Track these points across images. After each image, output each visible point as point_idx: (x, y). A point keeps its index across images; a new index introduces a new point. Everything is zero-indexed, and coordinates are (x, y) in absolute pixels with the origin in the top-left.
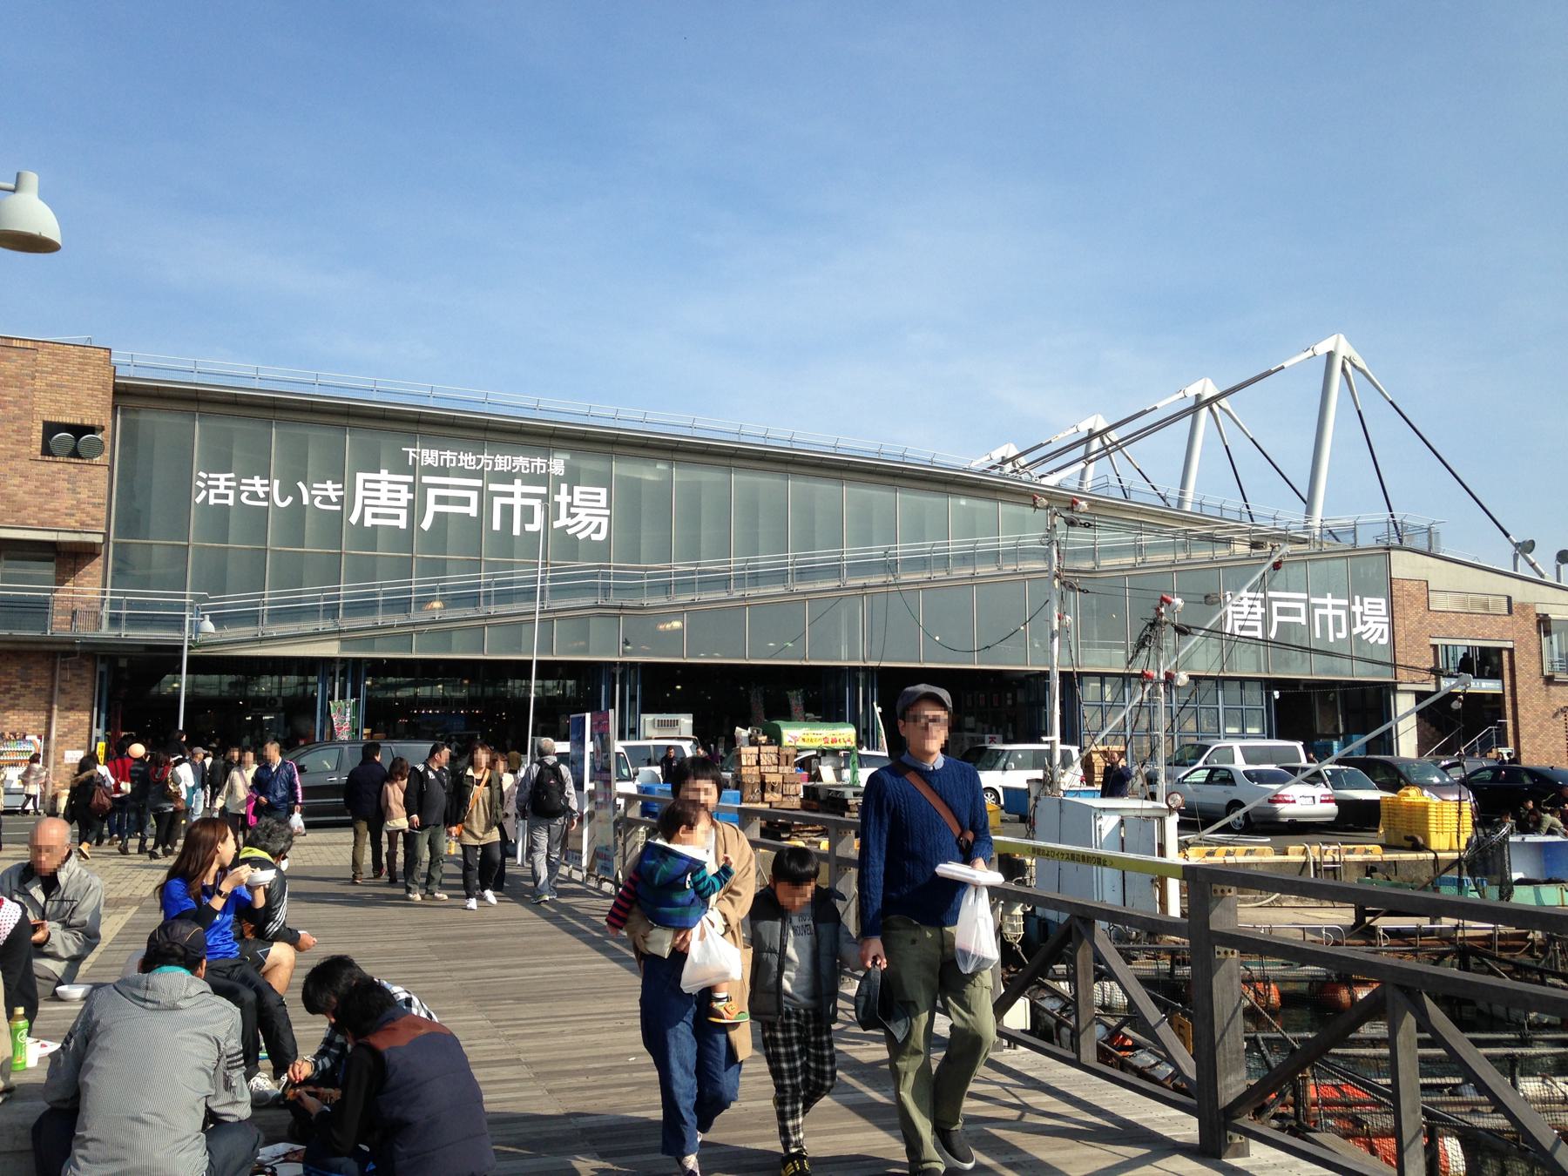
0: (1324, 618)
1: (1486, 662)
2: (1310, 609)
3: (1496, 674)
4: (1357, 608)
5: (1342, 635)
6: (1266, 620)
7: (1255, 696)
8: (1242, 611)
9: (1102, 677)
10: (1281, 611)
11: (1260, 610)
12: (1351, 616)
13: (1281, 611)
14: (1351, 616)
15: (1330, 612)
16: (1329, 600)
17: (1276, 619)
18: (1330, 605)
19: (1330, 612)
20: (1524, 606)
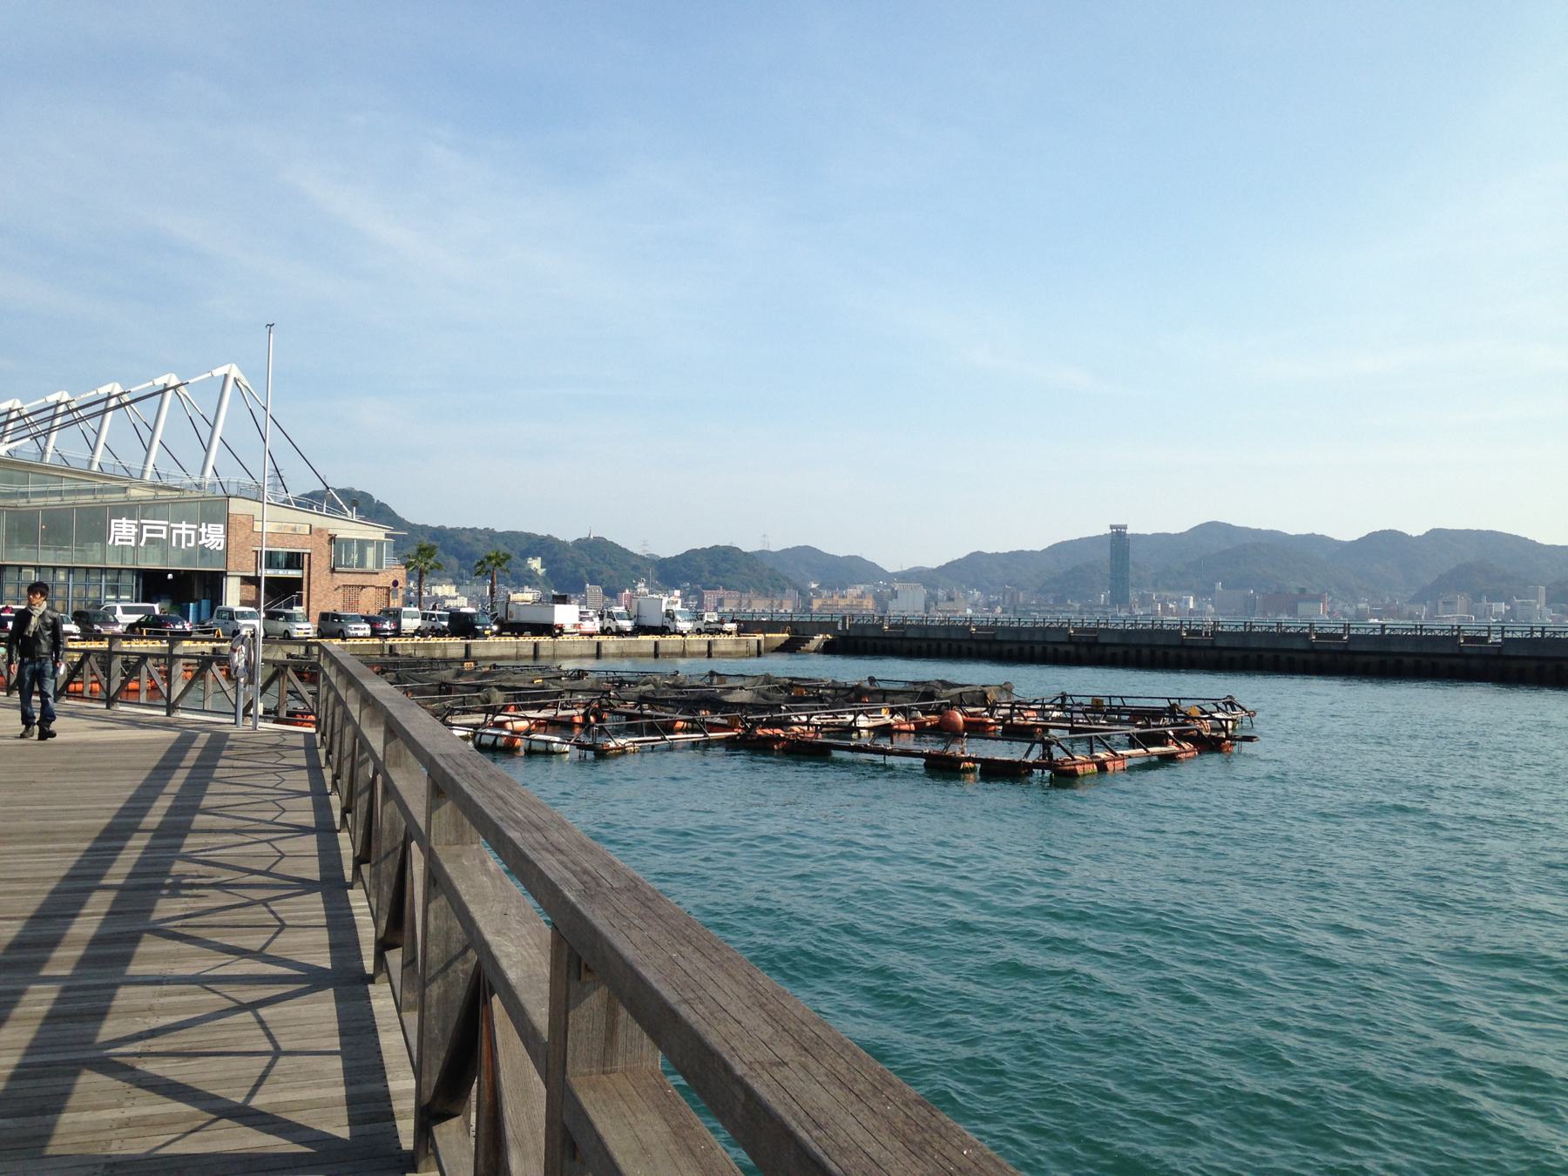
0: (179, 536)
1: (294, 560)
2: (170, 530)
3: (299, 567)
4: (203, 530)
5: (191, 545)
6: (139, 536)
7: (129, 580)
8: (123, 531)
9: (55, 568)
10: (149, 531)
11: (134, 530)
12: (198, 536)
13: (149, 531)
14: (198, 536)
15: (184, 532)
16: (184, 525)
17: (145, 535)
18: (184, 528)
19: (184, 532)
20: (320, 530)
